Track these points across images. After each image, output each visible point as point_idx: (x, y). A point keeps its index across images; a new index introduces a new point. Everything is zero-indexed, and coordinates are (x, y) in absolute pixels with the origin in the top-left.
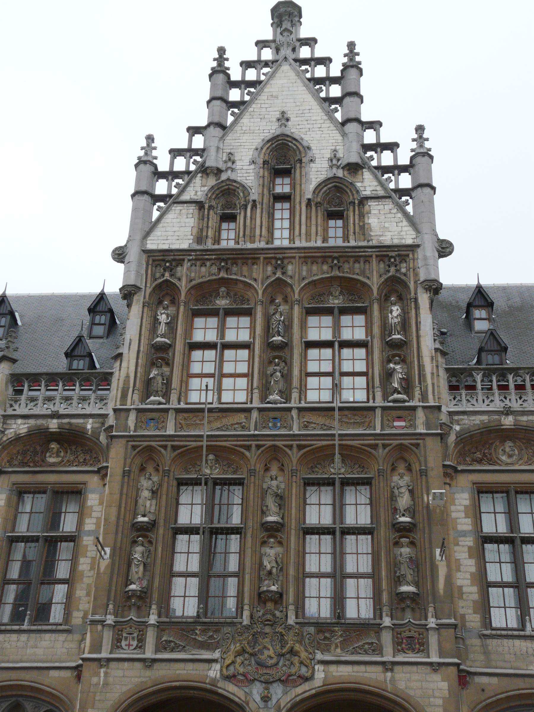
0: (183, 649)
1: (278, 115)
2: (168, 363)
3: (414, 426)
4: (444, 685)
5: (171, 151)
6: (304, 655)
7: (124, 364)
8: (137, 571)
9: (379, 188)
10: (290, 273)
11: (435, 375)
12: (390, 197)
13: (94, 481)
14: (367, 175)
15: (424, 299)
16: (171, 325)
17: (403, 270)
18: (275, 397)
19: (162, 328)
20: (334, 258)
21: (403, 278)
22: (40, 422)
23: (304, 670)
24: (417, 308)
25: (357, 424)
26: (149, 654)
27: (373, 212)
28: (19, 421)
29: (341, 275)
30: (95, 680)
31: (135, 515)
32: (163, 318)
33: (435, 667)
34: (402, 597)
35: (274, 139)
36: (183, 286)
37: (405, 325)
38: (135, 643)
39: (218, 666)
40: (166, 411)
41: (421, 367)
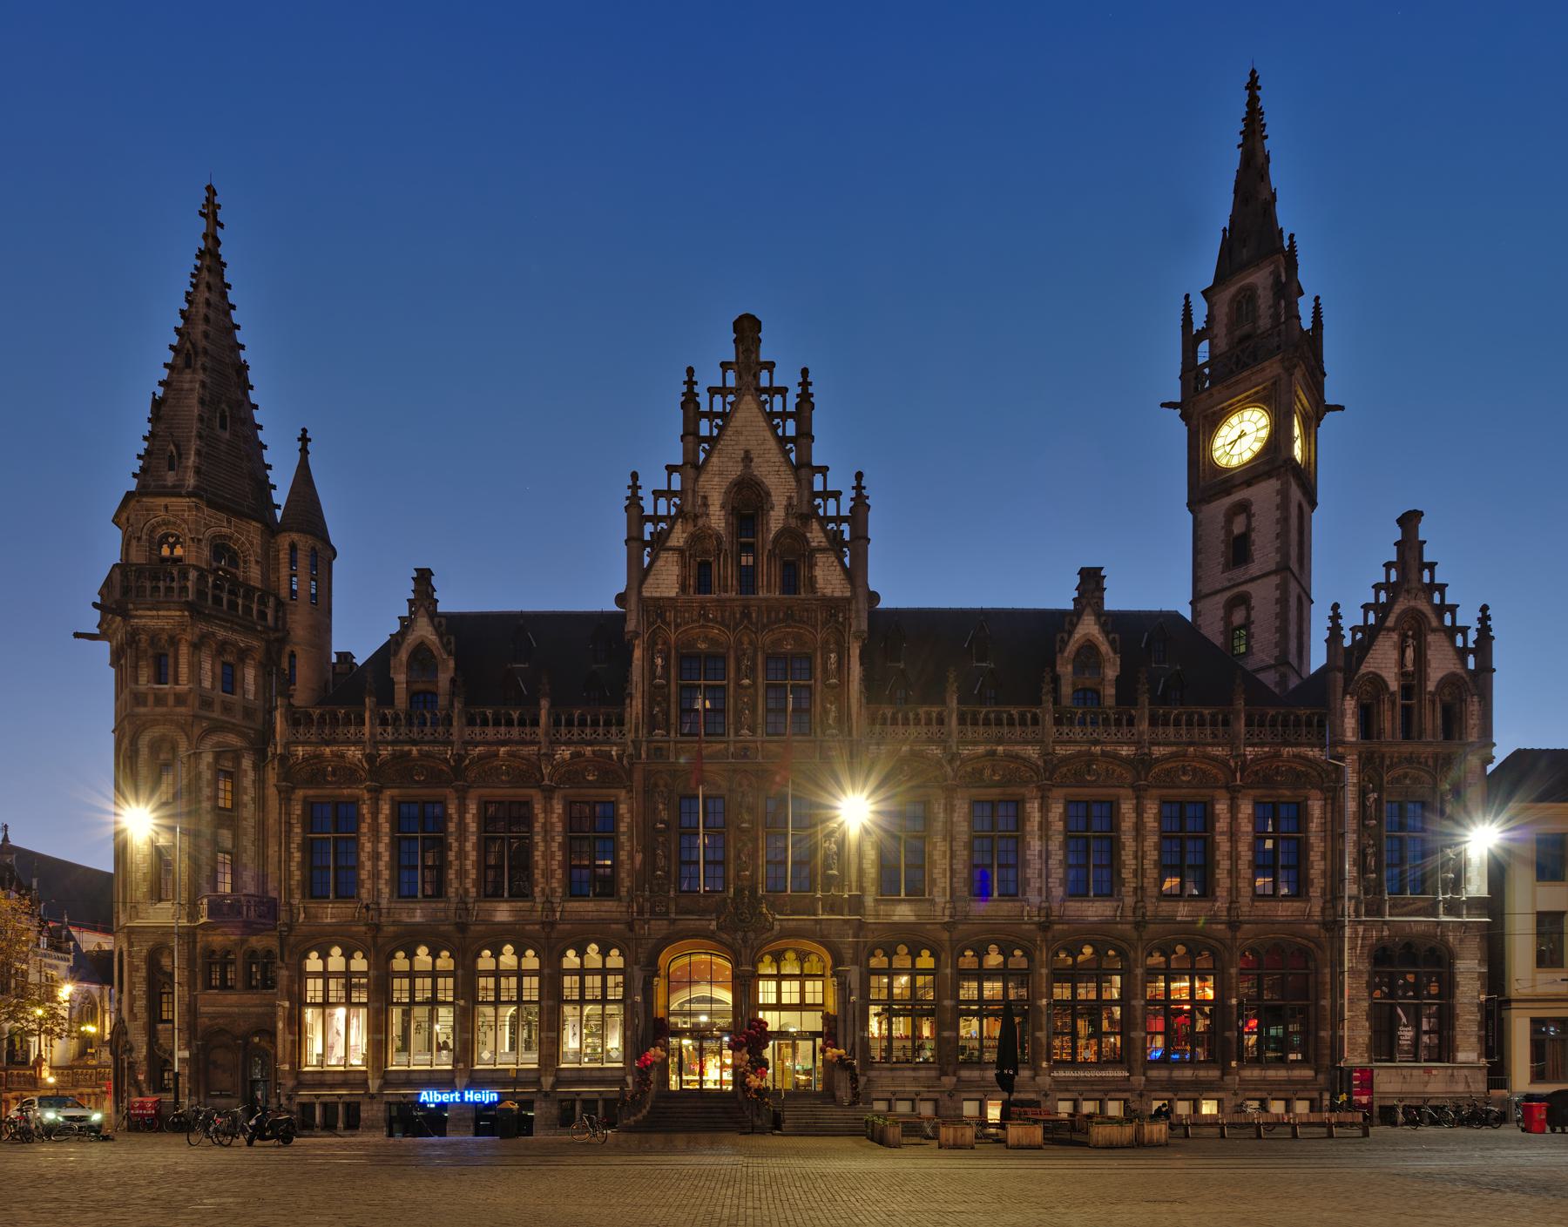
2: (667, 699)
5: (654, 492)
7: (634, 703)
8: (662, 862)
10: (754, 620)
11: (859, 714)
16: (666, 668)
17: (841, 619)
18: (745, 731)
21: (840, 627)
26: (673, 916)
30: (642, 932)
32: (659, 661)
39: (714, 923)
40: (669, 742)
41: (849, 707)
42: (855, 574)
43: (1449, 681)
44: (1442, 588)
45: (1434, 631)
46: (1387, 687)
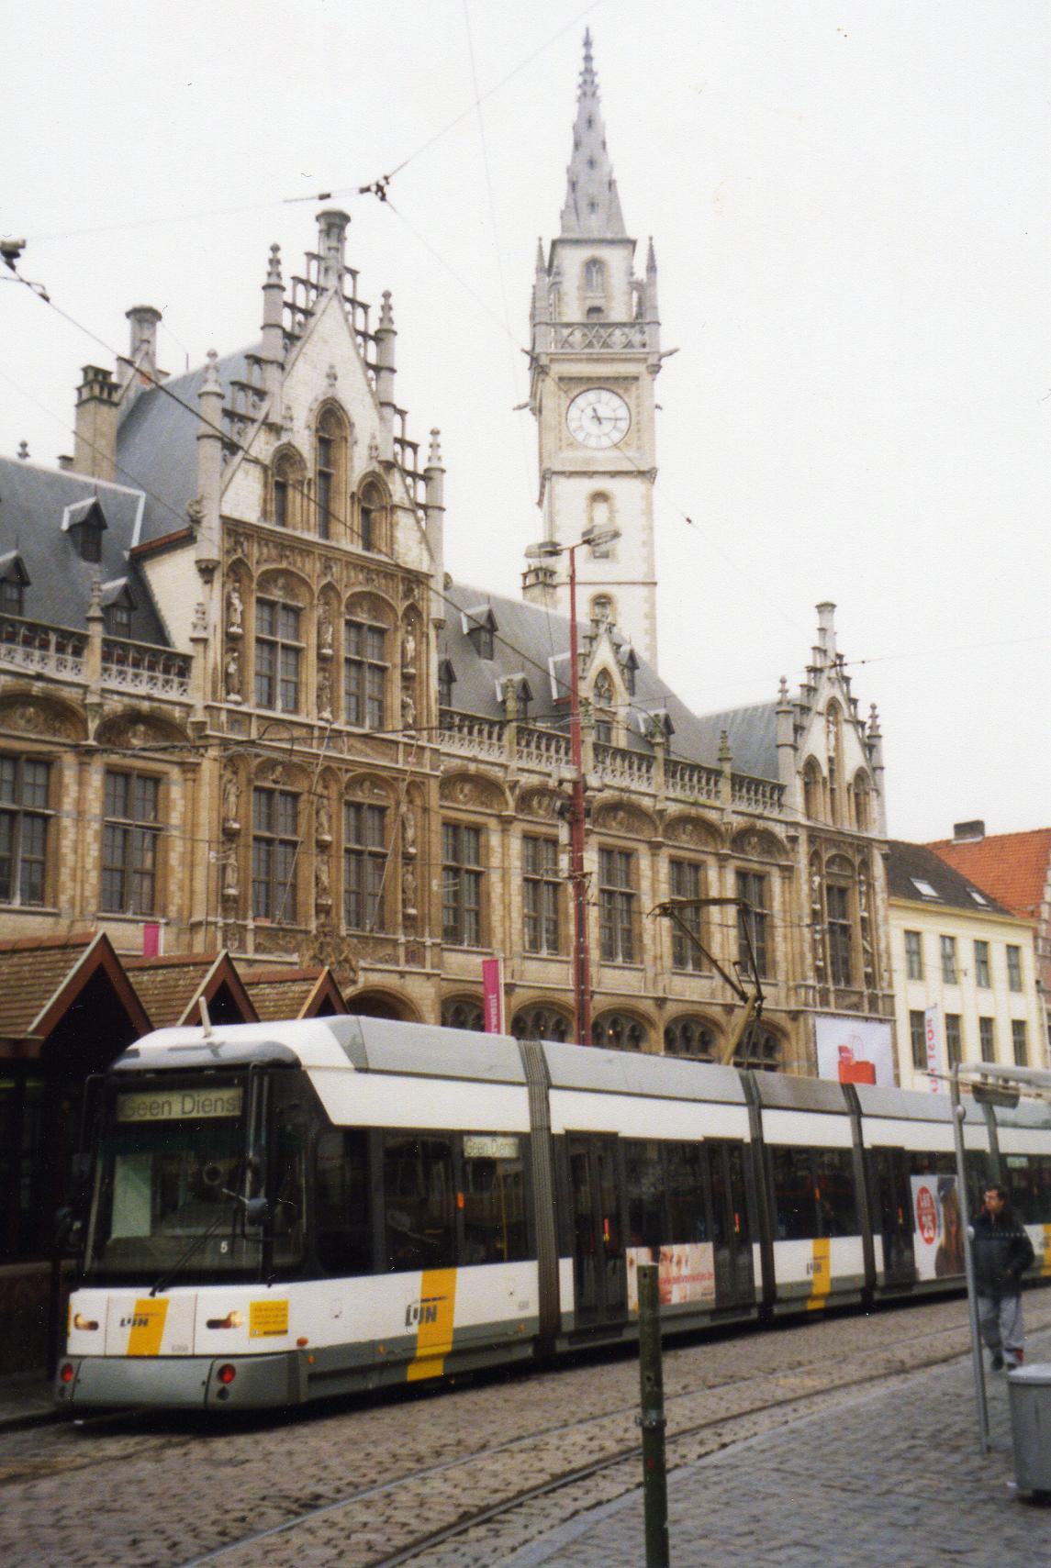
0: (270, 952)
1: (326, 369)
3: (419, 763)
4: (432, 990)
6: (354, 963)
8: (231, 877)
9: (405, 496)
12: (414, 512)
13: (175, 773)
14: (397, 476)
15: (432, 633)
18: (326, 715)
19: (237, 618)
20: (370, 571)
22: (134, 702)
23: (352, 975)
24: (428, 644)
25: (385, 754)
27: (401, 524)
28: (116, 697)
29: (375, 591)
31: (226, 820)
32: (236, 602)
33: (428, 976)
34: (407, 917)
35: (325, 402)
36: (257, 572)
37: (417, 657)
38: (236, 944)
42: (430, 543)
43: (861, 776)
44: (847, 680)
45: (846, 721)
46: (821, 771)
